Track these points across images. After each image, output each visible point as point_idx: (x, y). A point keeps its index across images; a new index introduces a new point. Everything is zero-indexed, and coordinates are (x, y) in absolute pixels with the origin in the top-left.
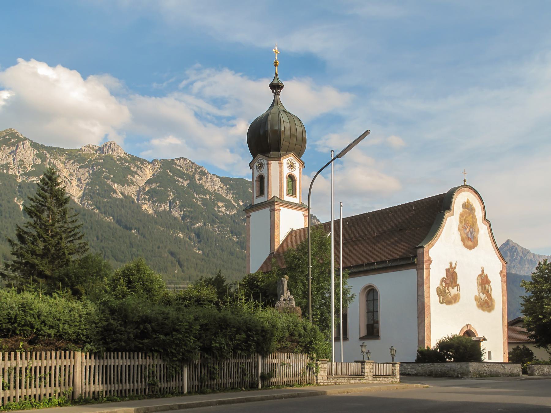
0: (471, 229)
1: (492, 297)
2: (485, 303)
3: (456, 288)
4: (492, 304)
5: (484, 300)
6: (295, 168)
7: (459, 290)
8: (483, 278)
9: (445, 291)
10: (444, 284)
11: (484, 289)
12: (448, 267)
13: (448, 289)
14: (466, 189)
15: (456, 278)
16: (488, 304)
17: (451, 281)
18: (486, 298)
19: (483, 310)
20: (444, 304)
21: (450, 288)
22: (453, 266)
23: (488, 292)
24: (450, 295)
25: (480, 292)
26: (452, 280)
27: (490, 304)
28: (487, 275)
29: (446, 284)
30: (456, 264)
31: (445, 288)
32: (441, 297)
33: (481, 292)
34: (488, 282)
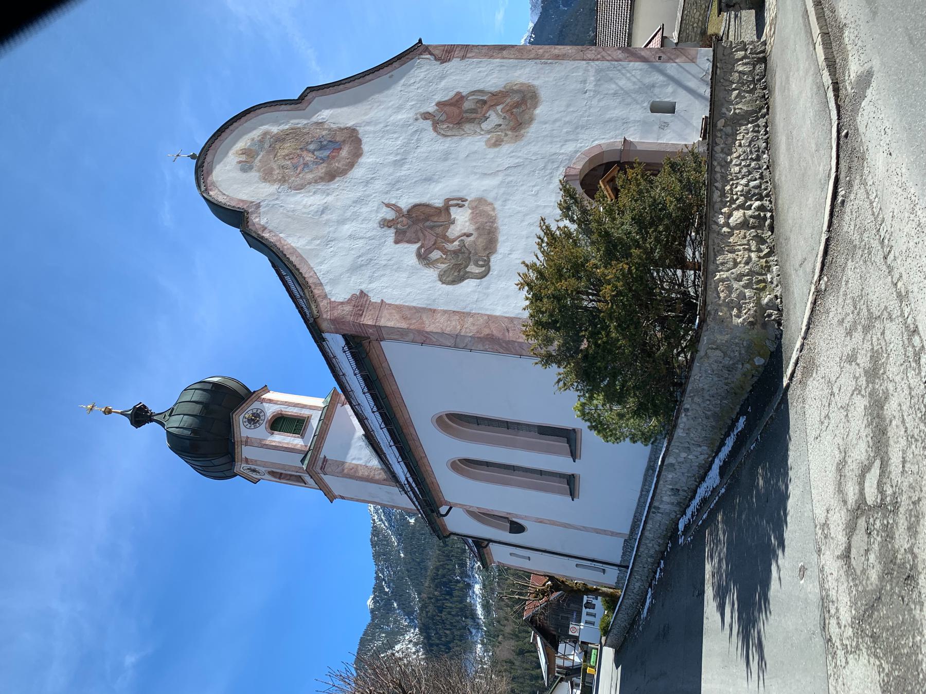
0: (312, 147)
1: (501, 92)
2: (512, 113)
3: (455, 213)
4: (516, 92)
5: (504, 118)
6: (261, 413)
7: (460, 202)
8: (444, 118)
9: (456, 253)
10: (436, 254)
11: (473, 116)
12: (391, 233)
13: (453, 241)
14: (208, 159)
15: (428, 210)
16: (517, 105)
17: (432, 228)
18: (499, 108)
19: (531, 120)
20: (493, 259)
21: (454, 231)
22: (390, 215)
23: (484, 102)
24: (469, 235)
25: (478, 130)
26: (428, 224)
27: (517, 98)
28: (439, 104)
29: (436, 247)
30: (388, 205)
31: (445, 252)
32: (472, 268)
33: (479, 124)
34: (459, 99)
